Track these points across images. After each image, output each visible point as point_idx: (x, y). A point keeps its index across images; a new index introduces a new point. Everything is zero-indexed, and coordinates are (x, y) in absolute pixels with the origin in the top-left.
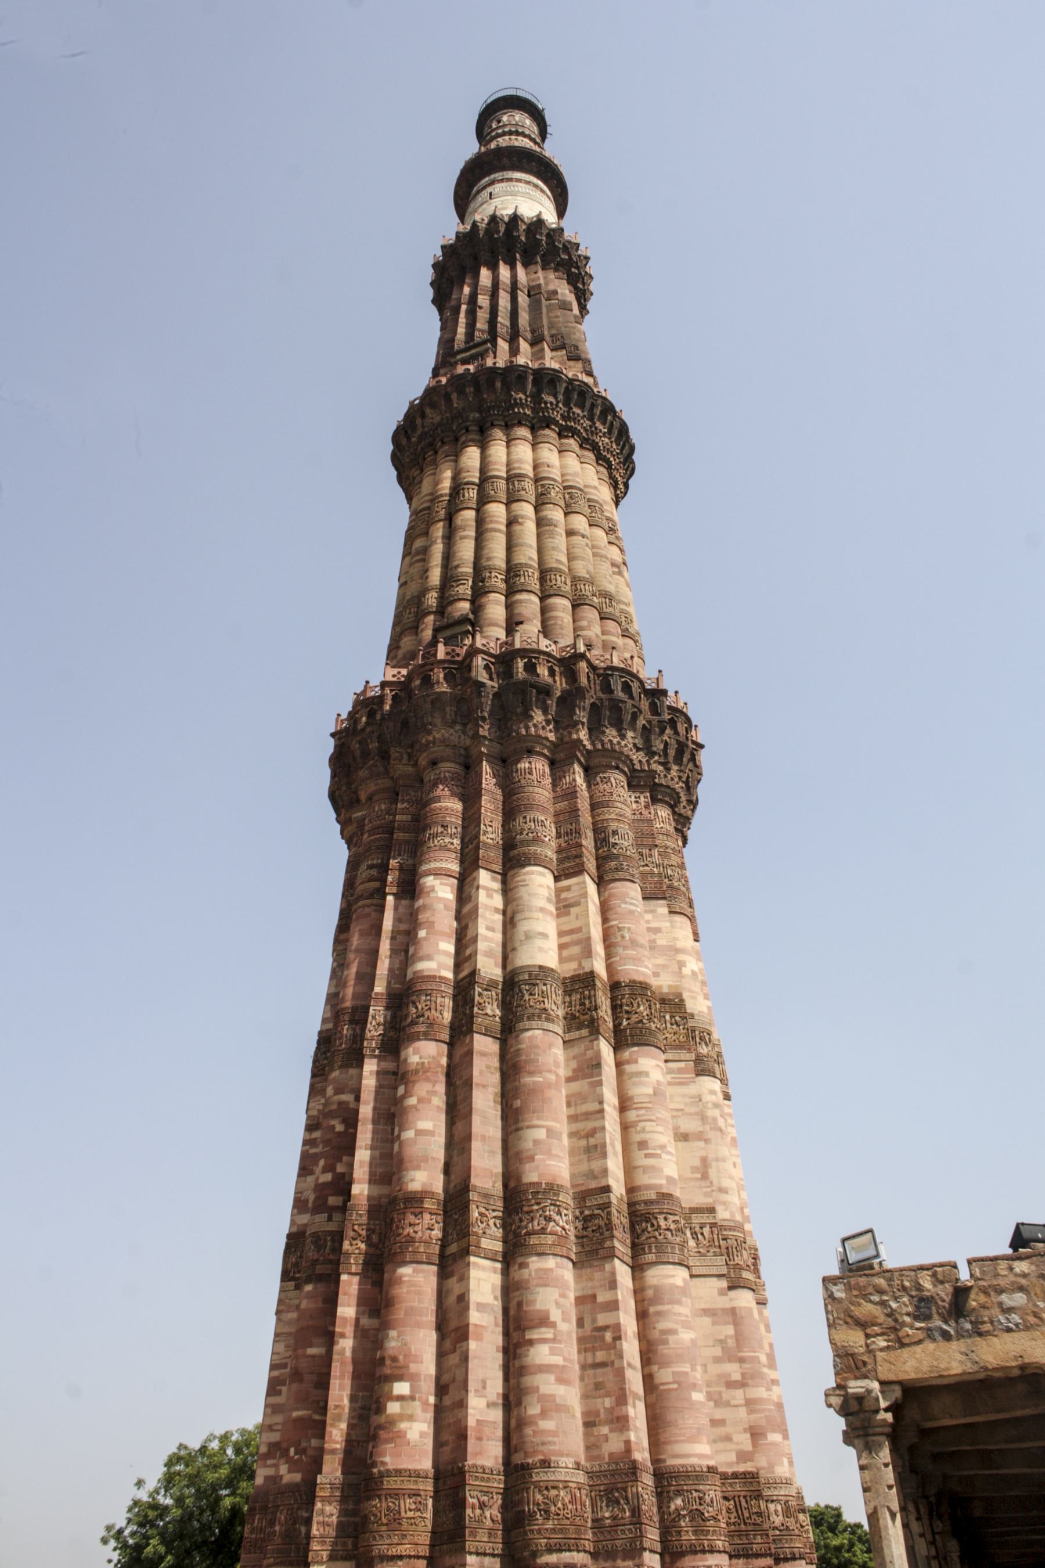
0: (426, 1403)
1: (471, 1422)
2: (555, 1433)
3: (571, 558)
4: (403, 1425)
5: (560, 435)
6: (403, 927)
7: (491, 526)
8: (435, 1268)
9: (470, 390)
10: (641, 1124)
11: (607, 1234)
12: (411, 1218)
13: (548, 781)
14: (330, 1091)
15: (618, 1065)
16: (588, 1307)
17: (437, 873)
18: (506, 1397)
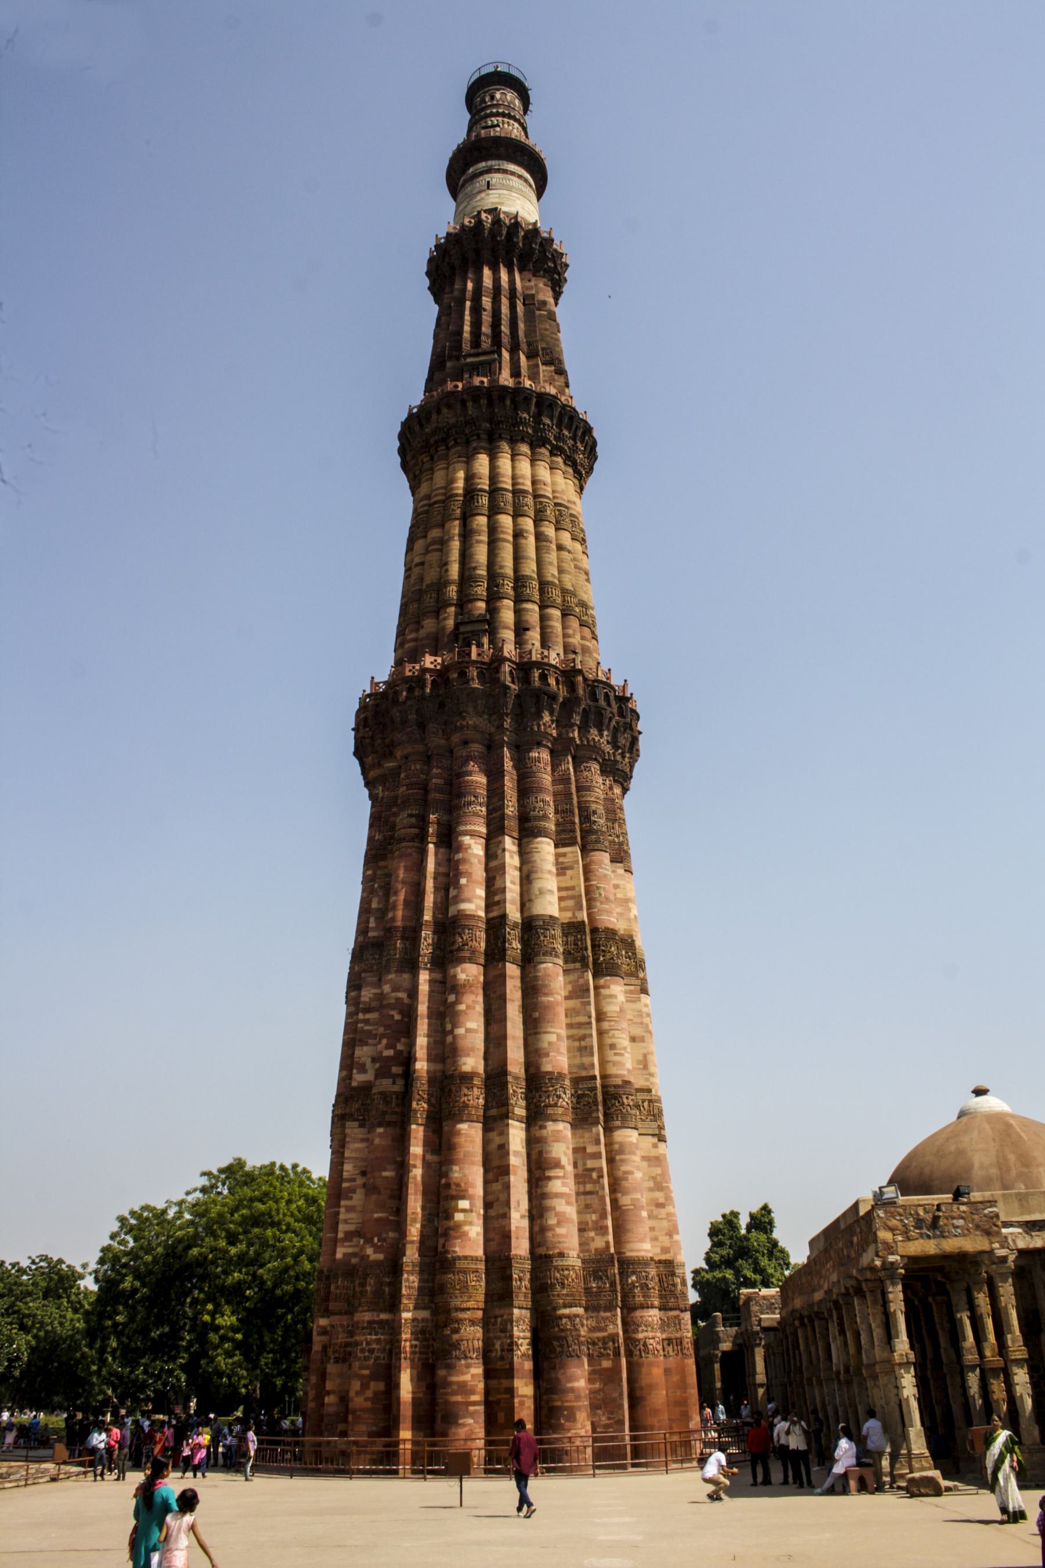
0: (479, 1214)
1: (513, 1228)
2: (566, 1236)
3: (561, 571)
4: (466, 1228)
5: (552, 454)
6: (442, 870)
7: (502, 536)
8: (480, 1125)
9: (484, 402)
10: (612, 1032)
11: (594, 1108)
12: (466, 1091)
13: (549, 768)
14: (387, 988)
15: (596, 988)
16: (580, 1155)
17: (473, 834)
18: (530, 1211)
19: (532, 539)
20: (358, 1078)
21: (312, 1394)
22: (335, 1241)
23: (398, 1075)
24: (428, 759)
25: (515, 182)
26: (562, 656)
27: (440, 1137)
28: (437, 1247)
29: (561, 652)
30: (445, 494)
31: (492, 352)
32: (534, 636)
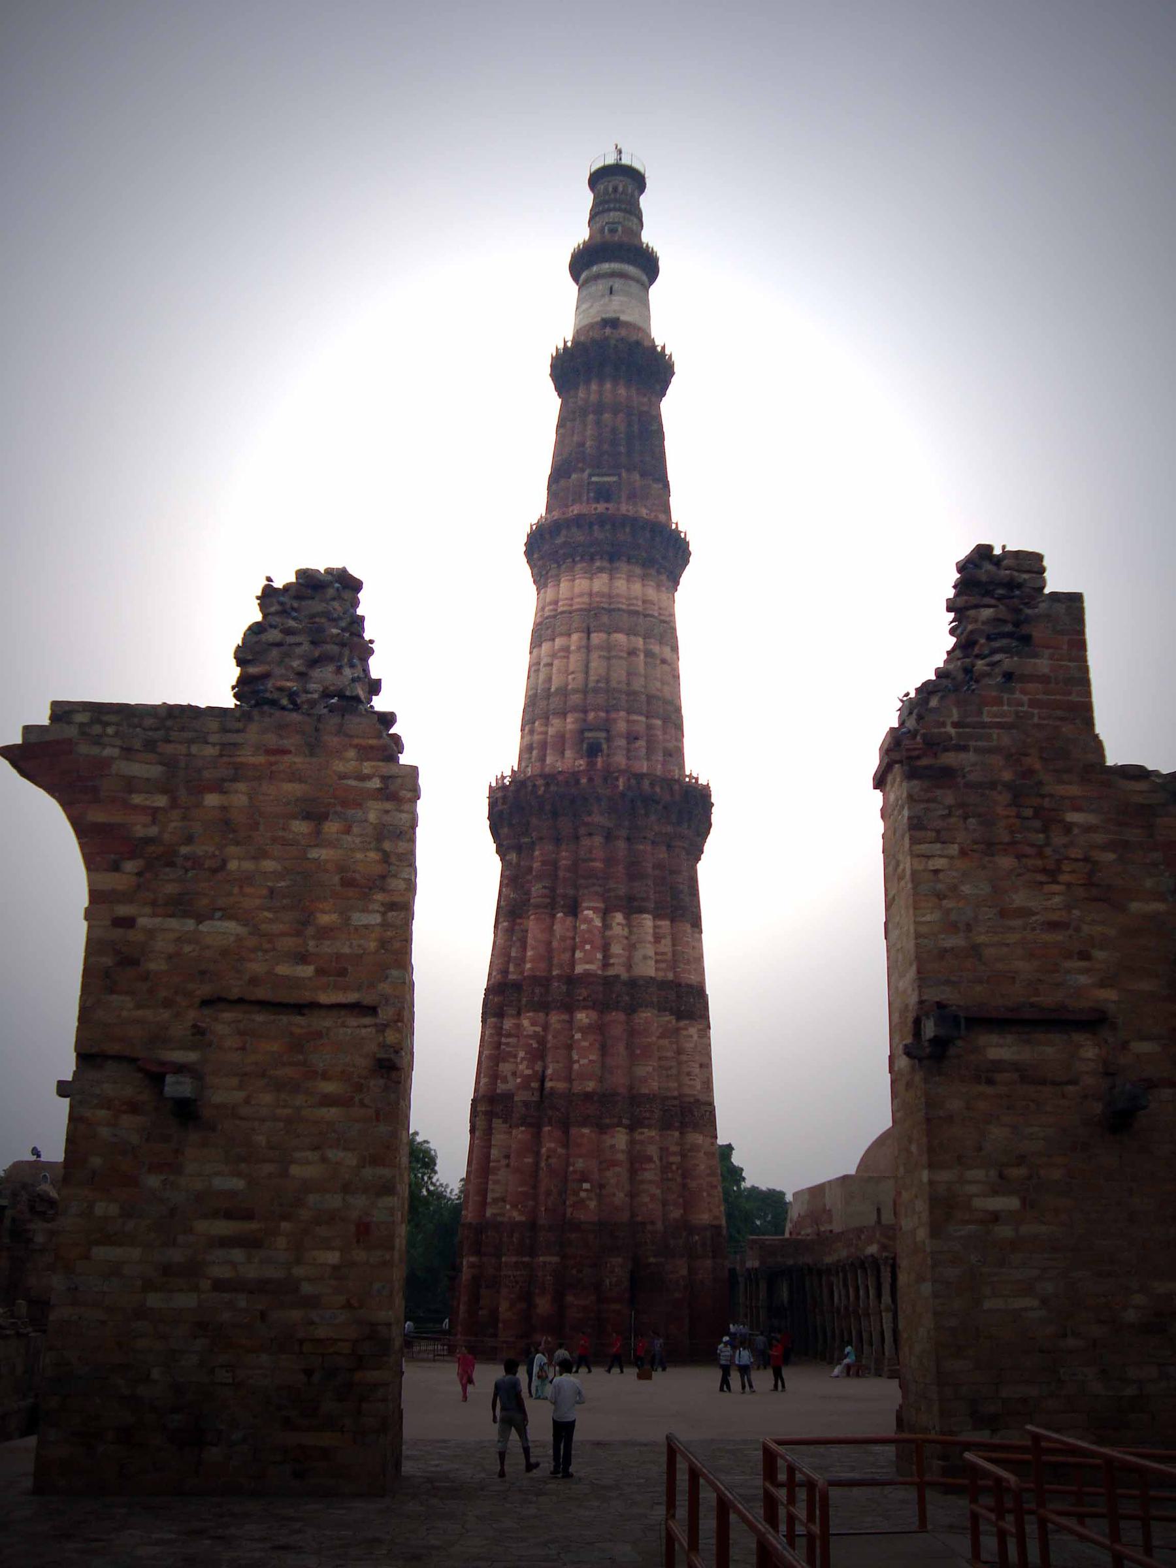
3: (663, 683)
5: (659, 572)
6: (570, 934)
9: (608, 527)
14: (526, 1023)
17: (594, 909)
19: (642, 656)
20: (501, 1087)
21: (462, 1308)
22: (484, 1204)
23: (533, 1089)
24: (558, 841)
25: (634, 287)
28: (565, 1214)
29: (660, 759)
30: (571, 605)
32: (641, 743)
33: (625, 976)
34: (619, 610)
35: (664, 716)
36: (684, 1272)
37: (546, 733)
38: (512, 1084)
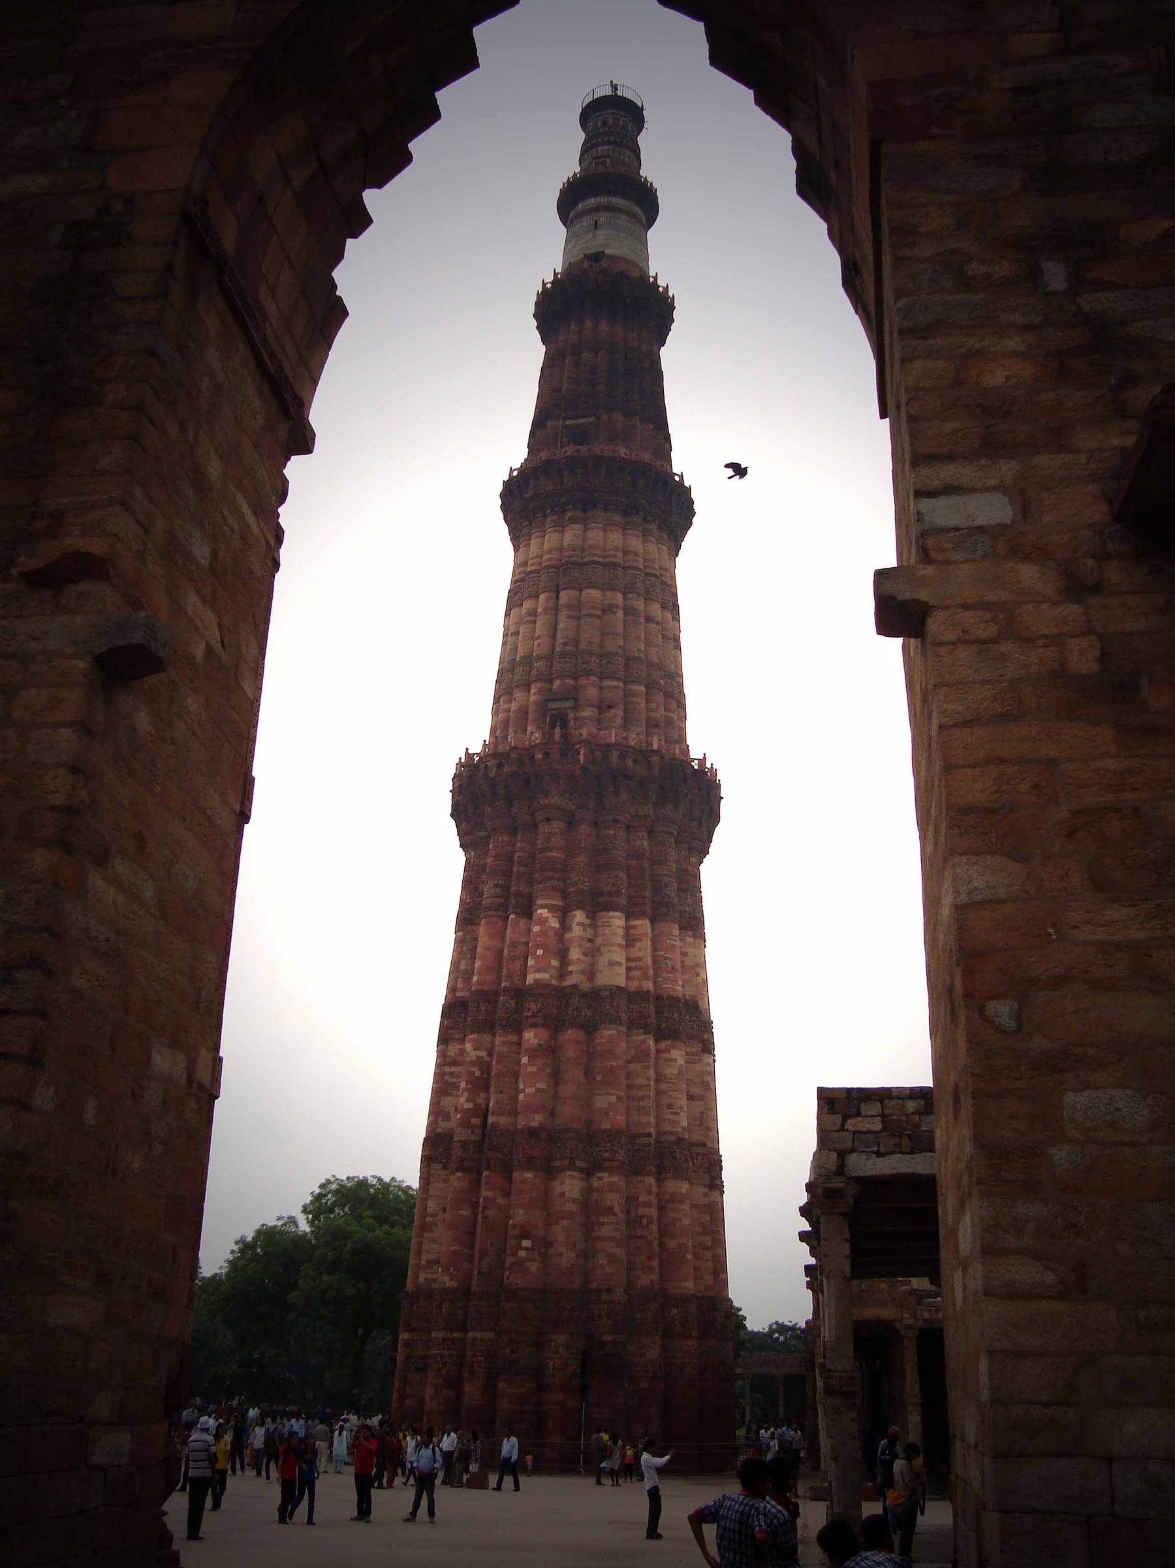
3: (648, 643)
4: (527, 1264)
6: (523, 940)
14: (468, 1046)
15: (658, 1051)
19: (620, 613)
20: (444, 1125)
23: (476, 1126)
24: (514, 832)
25: (623, 220)
26: (643, 737)
27: (510, 1184)
29: (642, 728)
31: (589, 416)
32: (618, 712)
33: (585, 985)
34: (595, 562)
35: (659, 685)
36: (654, 1353)
37: (509, 710)
38: (451, 1124)
